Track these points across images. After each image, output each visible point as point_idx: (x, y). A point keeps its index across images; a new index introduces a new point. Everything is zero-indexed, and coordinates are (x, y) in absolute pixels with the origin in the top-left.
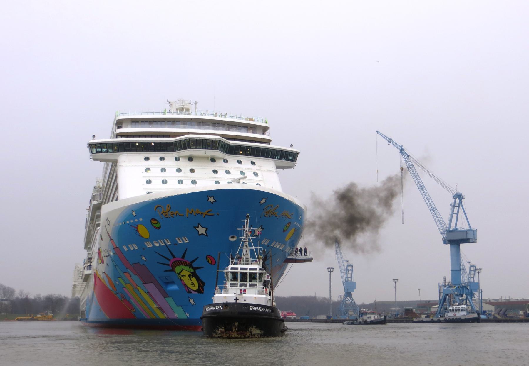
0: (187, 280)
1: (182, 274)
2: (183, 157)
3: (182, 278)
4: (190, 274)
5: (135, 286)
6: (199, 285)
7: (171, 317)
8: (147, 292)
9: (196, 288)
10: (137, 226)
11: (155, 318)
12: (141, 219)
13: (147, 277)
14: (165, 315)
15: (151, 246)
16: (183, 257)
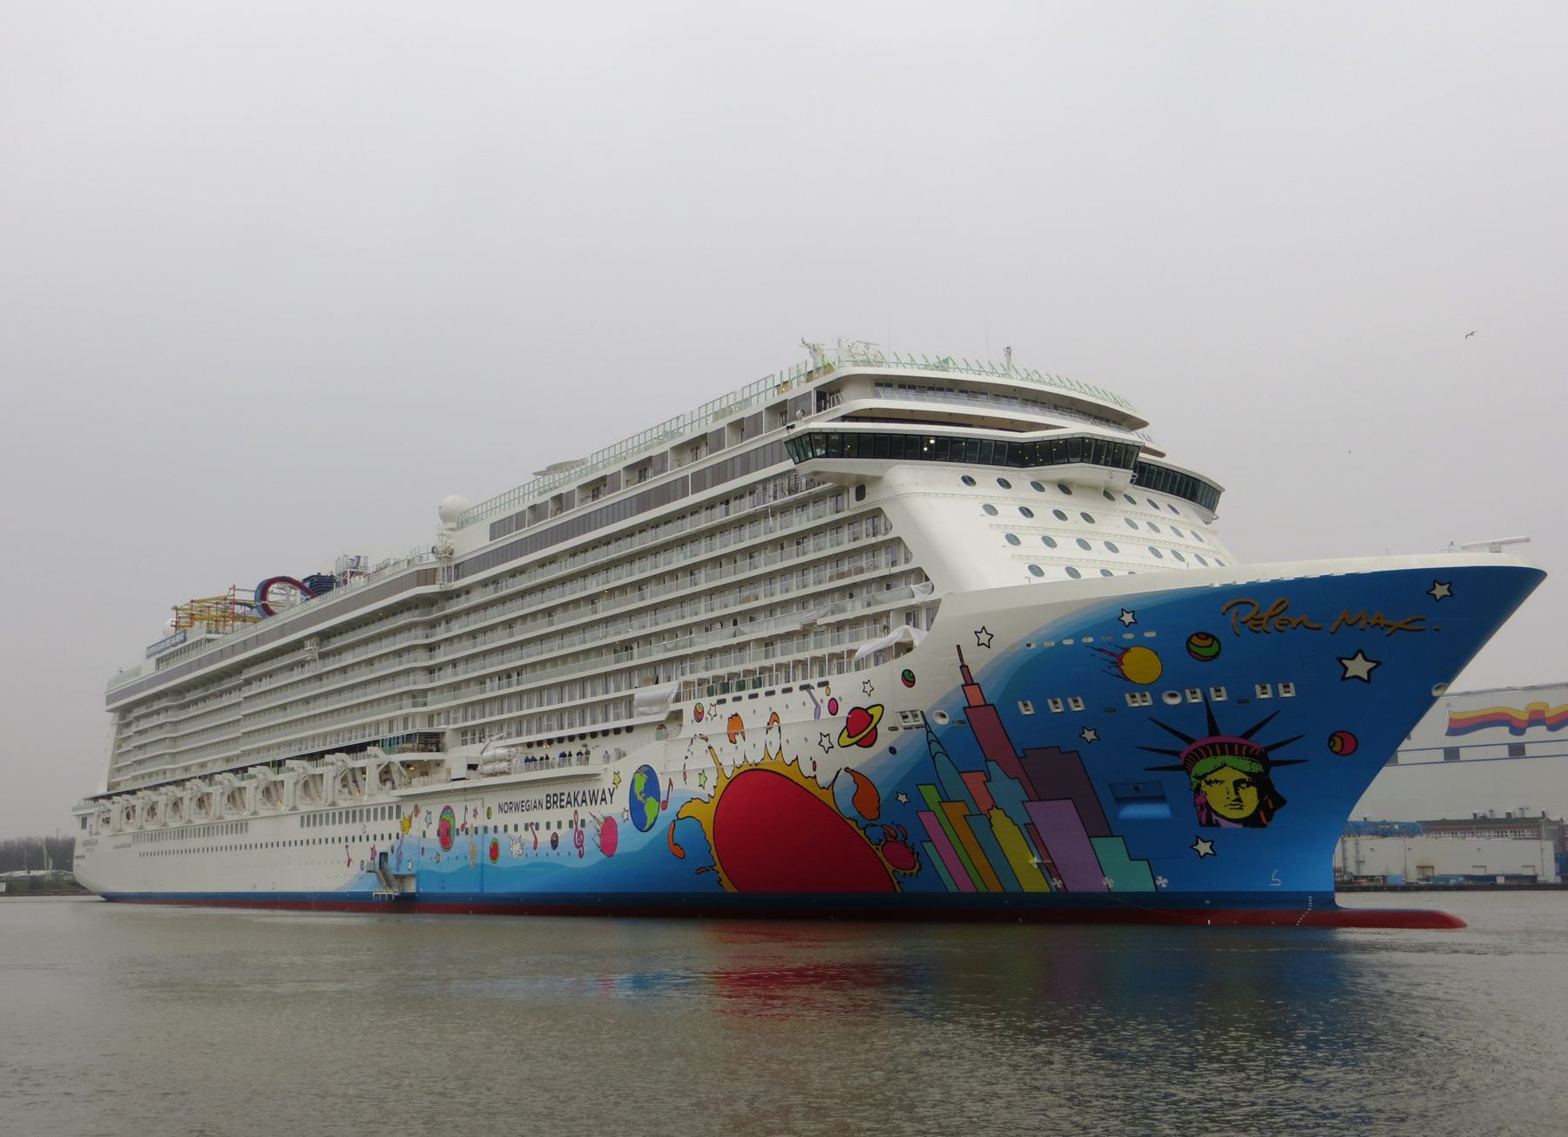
0: (1218, 798)
2: (1049, 482)
3: (1205, 788)
4: (1243, 776)
7: (1072, 888)
10: (1126, 650)
12: (1150, 634)
14: (1058, 883)
16: (1246, 736)
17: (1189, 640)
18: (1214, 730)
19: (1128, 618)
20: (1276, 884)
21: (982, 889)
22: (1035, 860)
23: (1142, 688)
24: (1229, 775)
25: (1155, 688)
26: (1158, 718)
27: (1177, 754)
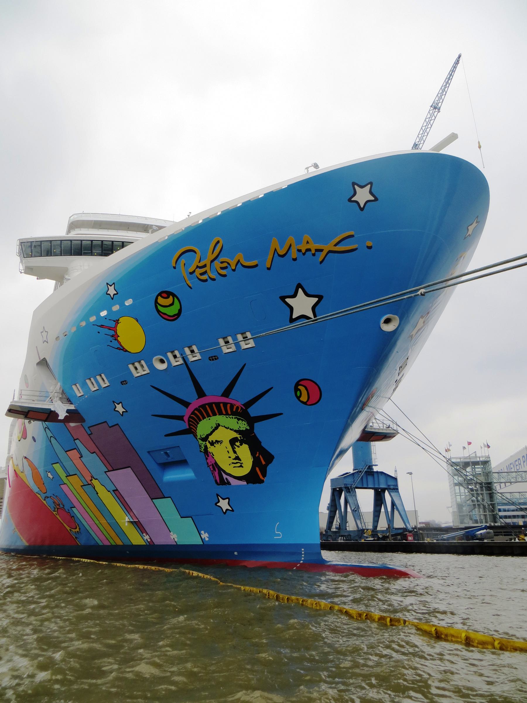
0: (222, 455)
1: (211, 439)
3: (211, 449)
4: (236, 435)
6: (256, 463)
7: (158, 541)
9: (246, 470)
10: (117, 322)
11: (119, 543)
12: (129, 302)
13: (117, 453)
14: (147, 537)
16: (227, 392)
17: (156, 302)
19: (112, 291)
20: (278, 537)
22: (127, 519)
23: (137, 358)
24: (225, 435)
26: (155, 384)
27: (180, 418)
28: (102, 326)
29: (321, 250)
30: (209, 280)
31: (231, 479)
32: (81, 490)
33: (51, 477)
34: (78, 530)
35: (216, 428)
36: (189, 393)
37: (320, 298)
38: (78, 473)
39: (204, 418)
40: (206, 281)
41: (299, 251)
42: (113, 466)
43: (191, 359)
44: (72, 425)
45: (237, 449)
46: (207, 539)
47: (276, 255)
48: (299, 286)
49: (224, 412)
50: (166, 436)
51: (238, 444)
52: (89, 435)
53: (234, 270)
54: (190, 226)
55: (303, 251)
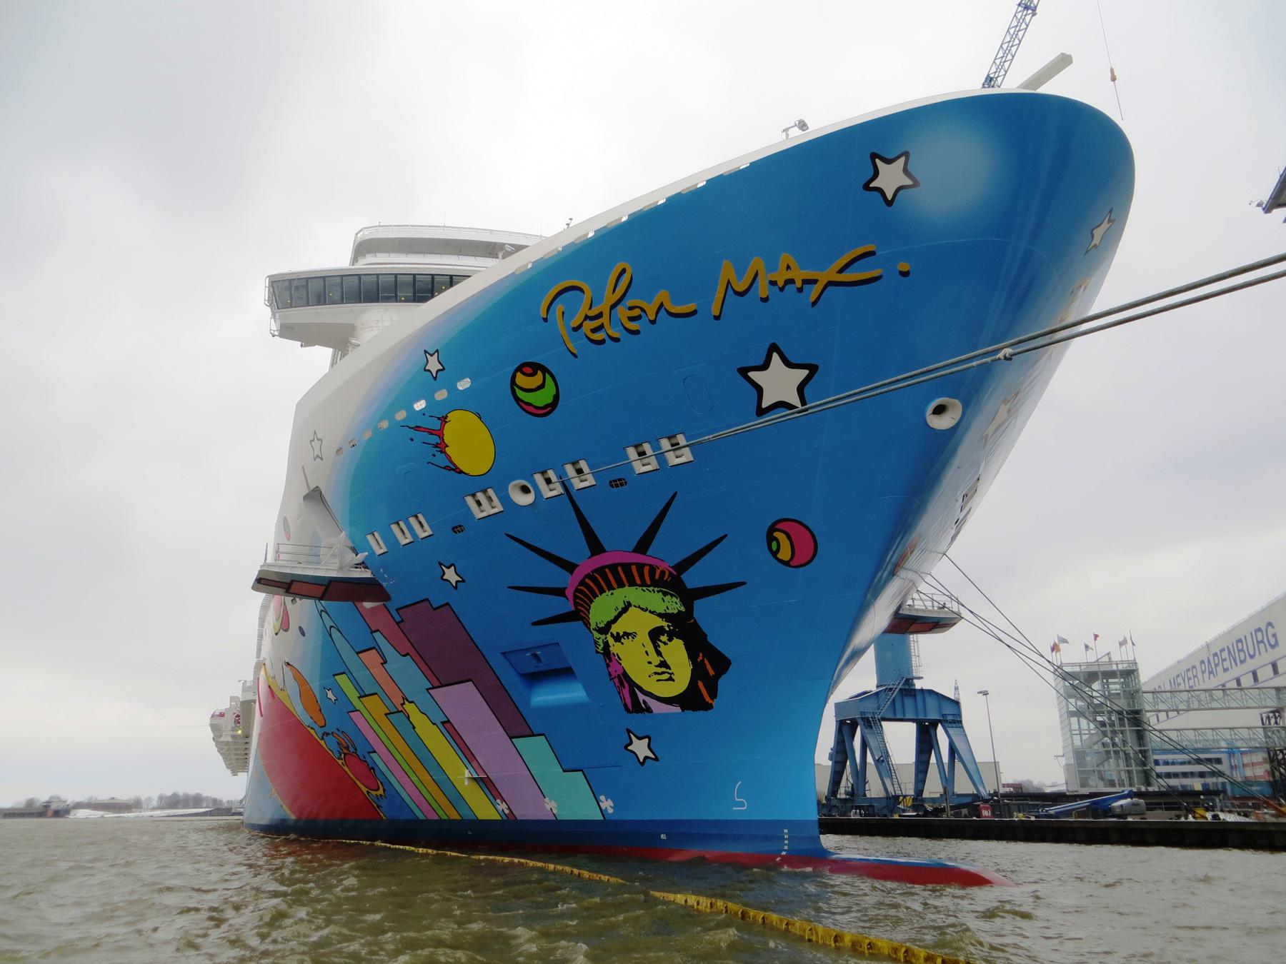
0: (635, 659)
1: (615, 629)
3: (615, 648)
5: (398, 701)
7: (523, 813)
8: (440, 718)
10: (444, 420)
11: (454, 816)
12: (464, 384)
15: (496, 510)
16: (643, 545)
18: (595, 546)
19: (434, 365)
20: (740, 808)
21: (444, 817)
22: (467, 774)
23: (480, 484)
24: (640, 623)
25: (494, 480)
27: (560, 592)
28: (417, 428)
29: (814, 282)
30: (608, 340)
31: (652, 703)
32: (385, 723)
33: (333, 698)
34: (381, 792)
35: (625, 610)
36: (574, 547)
37: (813, 369)
38: (379, 691)
39: (602, 591)
40: (602, 342)
41: (773, 283)
42: (440, 679)
43: (578, 484)
44: (368, 605)
45: (662, 648)
46: (610, 811)
47: (730, 292)
48: (774, 348)
49: (638, 582)
50: (535, 624)
51: (664, 638)
52: (398, 623)
53: (653, 322)
54: (573, 243)
55: (781, 284)
